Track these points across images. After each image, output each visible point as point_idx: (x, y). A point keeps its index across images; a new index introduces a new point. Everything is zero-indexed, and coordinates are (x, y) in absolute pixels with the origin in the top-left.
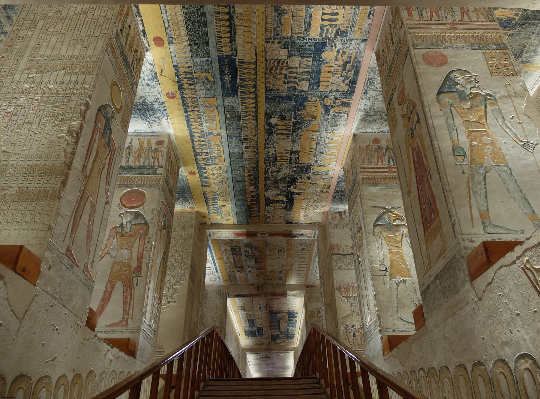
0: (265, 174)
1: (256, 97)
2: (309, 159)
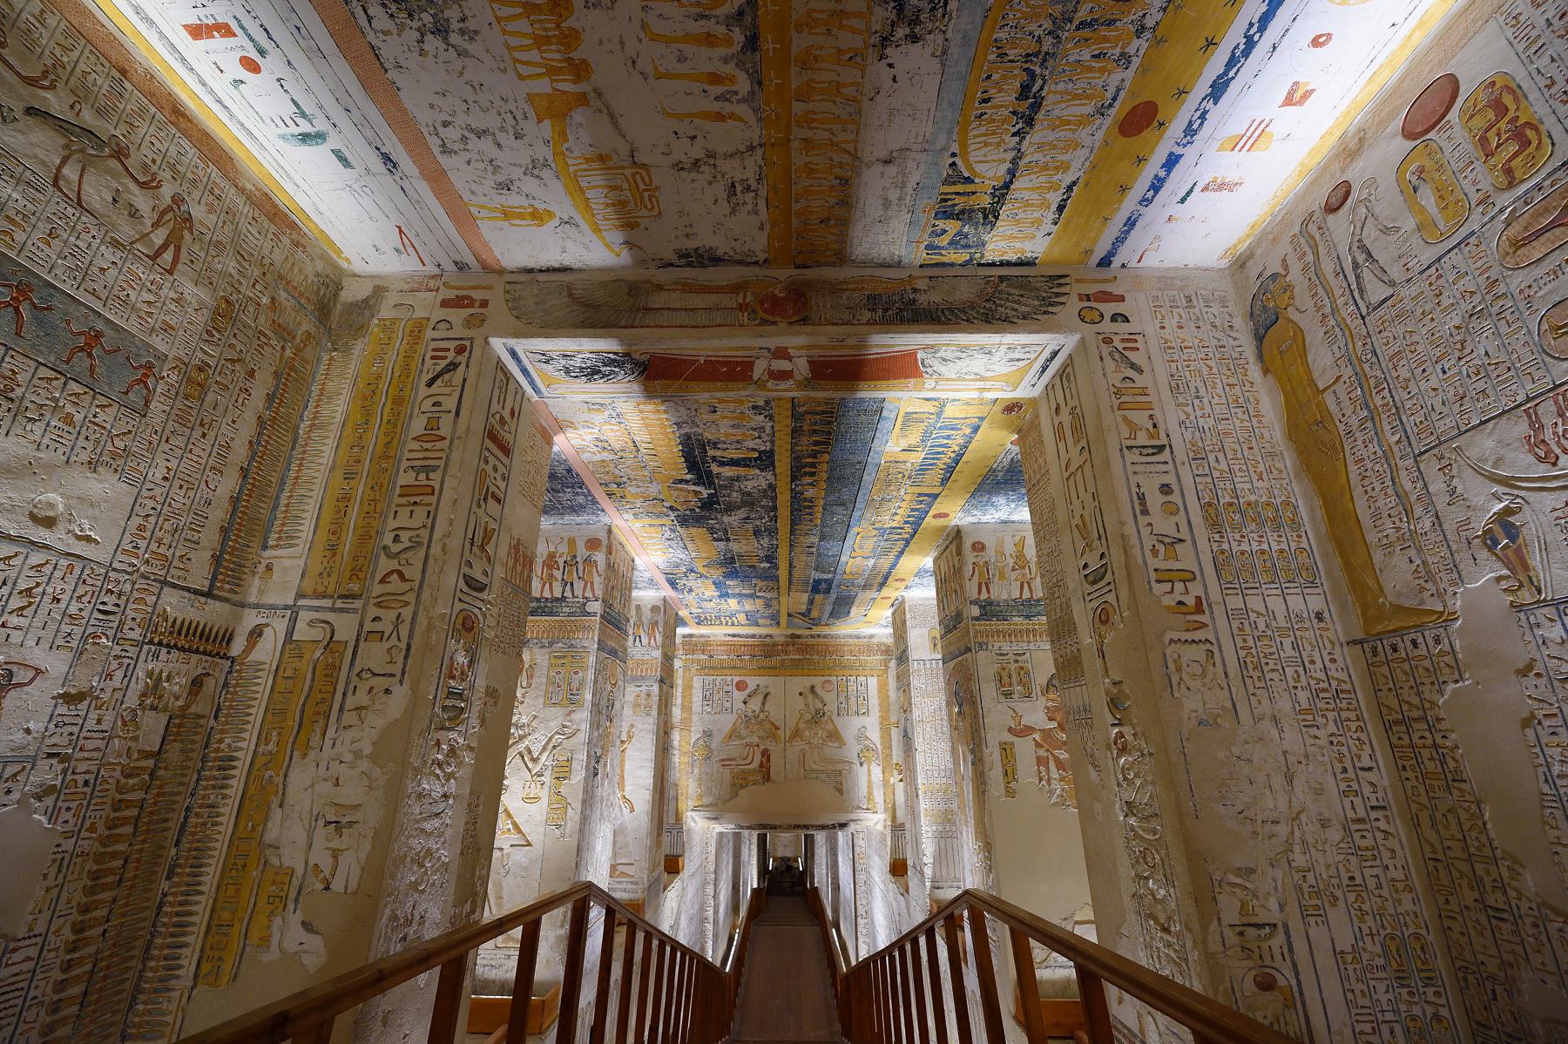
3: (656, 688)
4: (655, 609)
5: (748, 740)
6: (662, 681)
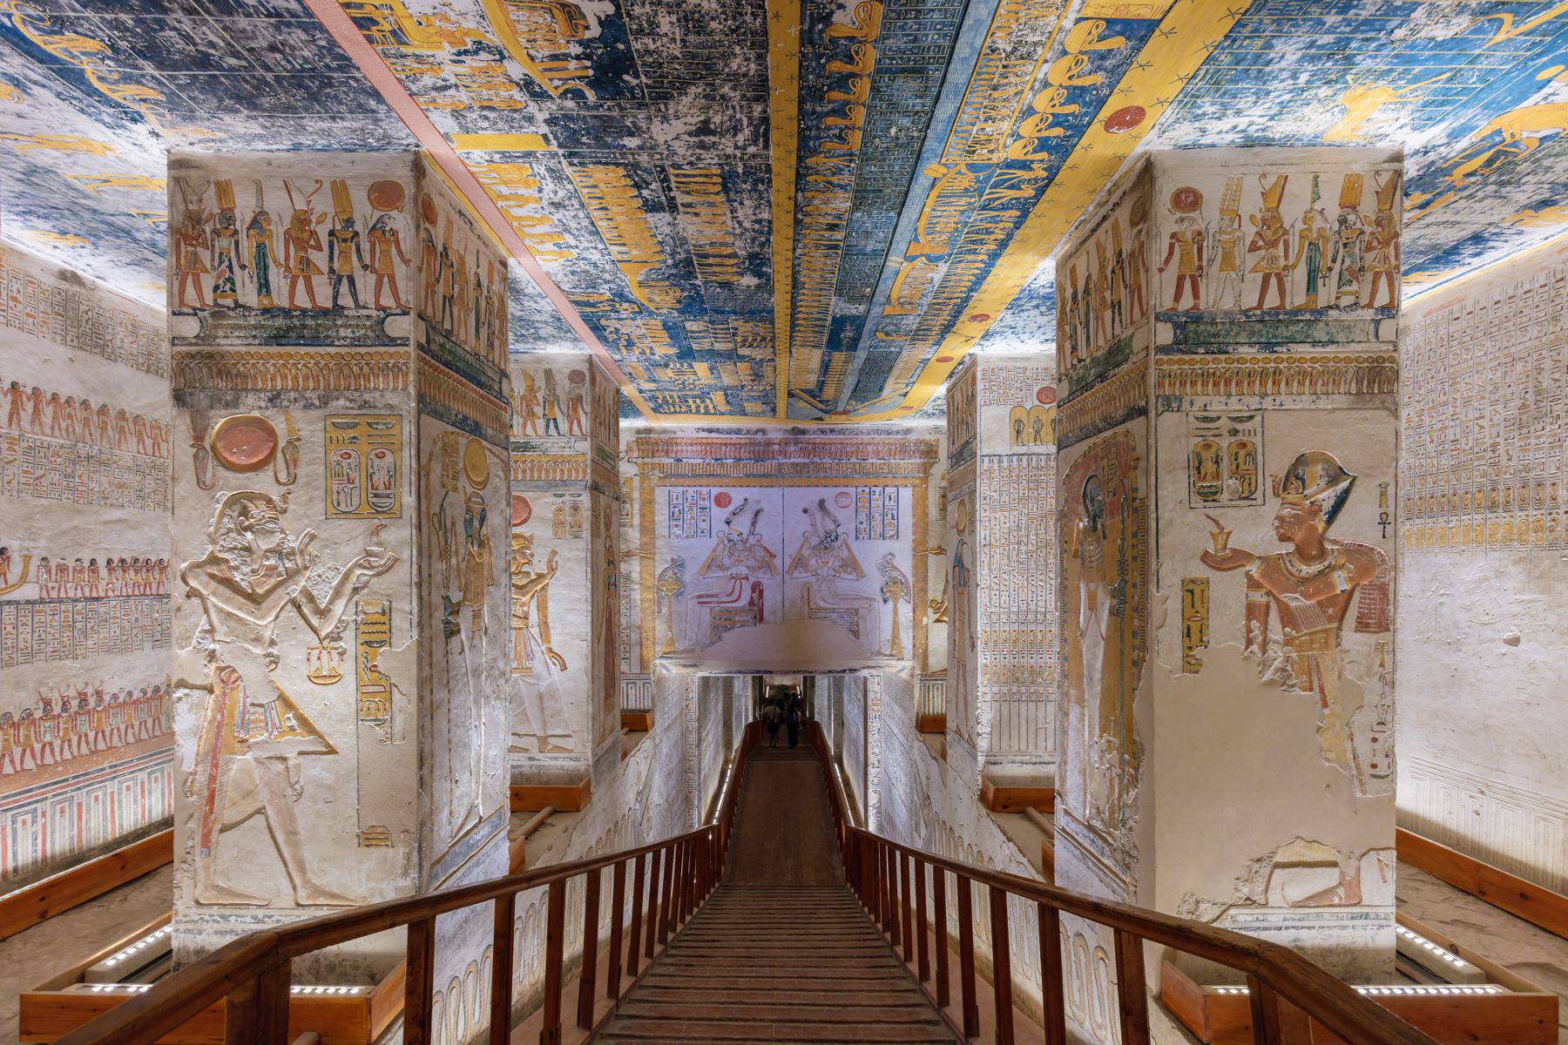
0: (765, 120)
1: (792, 315)
2: (591, 182)
3: (585, 499)
4: (575, 376)
5: (733, 571)
6: (595, 488)
